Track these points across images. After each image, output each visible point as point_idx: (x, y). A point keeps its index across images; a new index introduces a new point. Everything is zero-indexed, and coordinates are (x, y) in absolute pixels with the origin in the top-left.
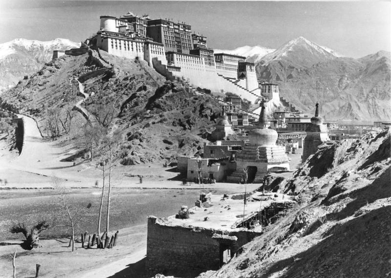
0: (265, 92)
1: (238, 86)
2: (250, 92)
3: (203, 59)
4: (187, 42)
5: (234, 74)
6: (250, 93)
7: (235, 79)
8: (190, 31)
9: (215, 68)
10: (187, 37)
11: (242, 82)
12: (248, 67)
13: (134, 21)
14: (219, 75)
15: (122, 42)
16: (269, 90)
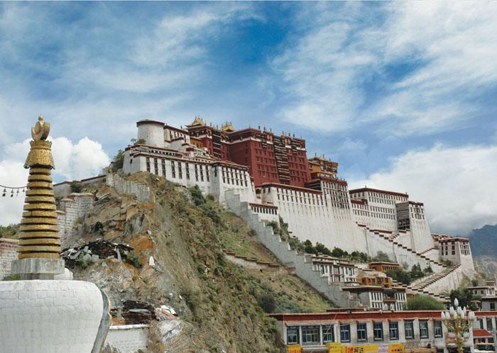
0: (447, 254)
1: (396, 243)
2: (418, 255)
3: (328, 196)
4: (299, 169)
5: (390, 224)
6: (419, 258)
7: (391, 233)
8: (303, 149)
9: (353, 215)
10: (298, 159)
11: (403, 238)
12: (412, 212)
13: (202, 134)
14: (360, 225)
15: (168, 163)
16: (453, 248)
